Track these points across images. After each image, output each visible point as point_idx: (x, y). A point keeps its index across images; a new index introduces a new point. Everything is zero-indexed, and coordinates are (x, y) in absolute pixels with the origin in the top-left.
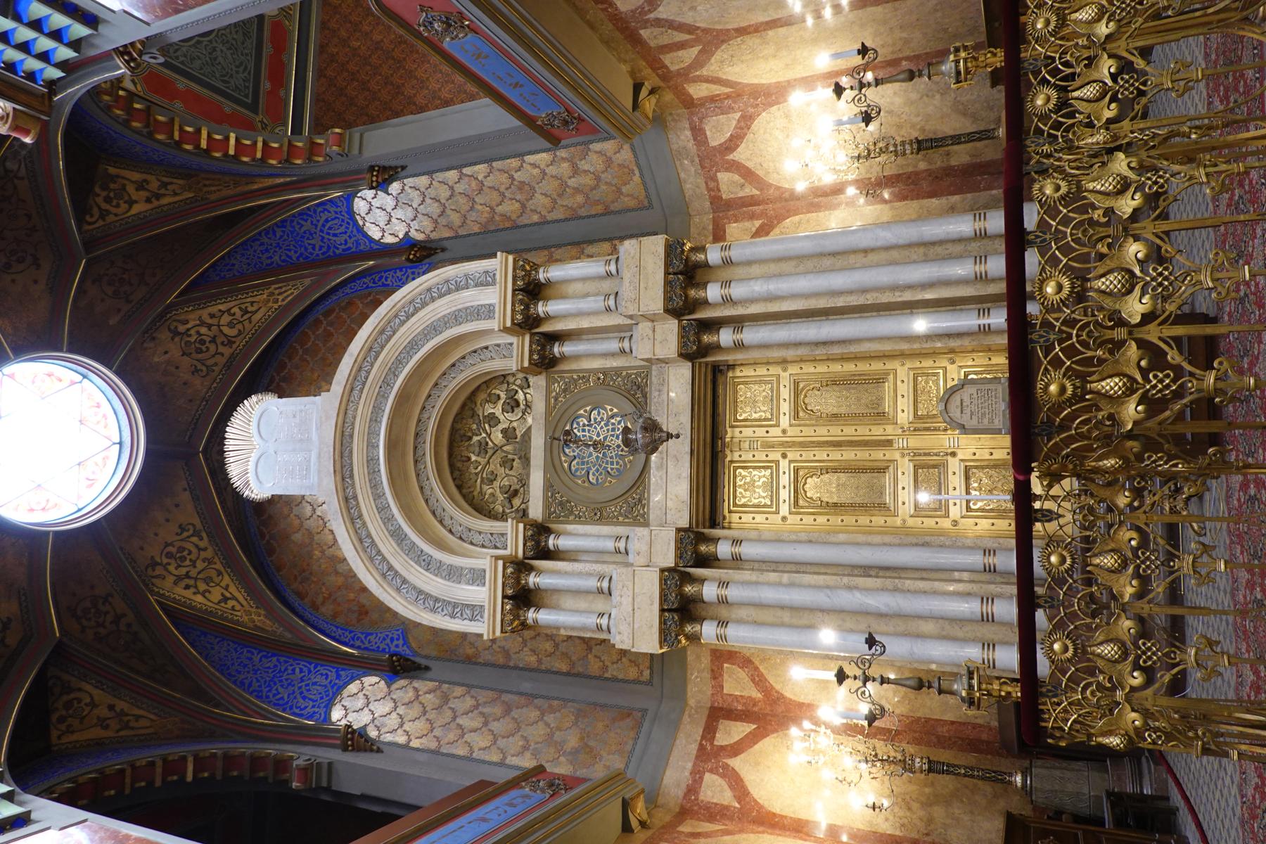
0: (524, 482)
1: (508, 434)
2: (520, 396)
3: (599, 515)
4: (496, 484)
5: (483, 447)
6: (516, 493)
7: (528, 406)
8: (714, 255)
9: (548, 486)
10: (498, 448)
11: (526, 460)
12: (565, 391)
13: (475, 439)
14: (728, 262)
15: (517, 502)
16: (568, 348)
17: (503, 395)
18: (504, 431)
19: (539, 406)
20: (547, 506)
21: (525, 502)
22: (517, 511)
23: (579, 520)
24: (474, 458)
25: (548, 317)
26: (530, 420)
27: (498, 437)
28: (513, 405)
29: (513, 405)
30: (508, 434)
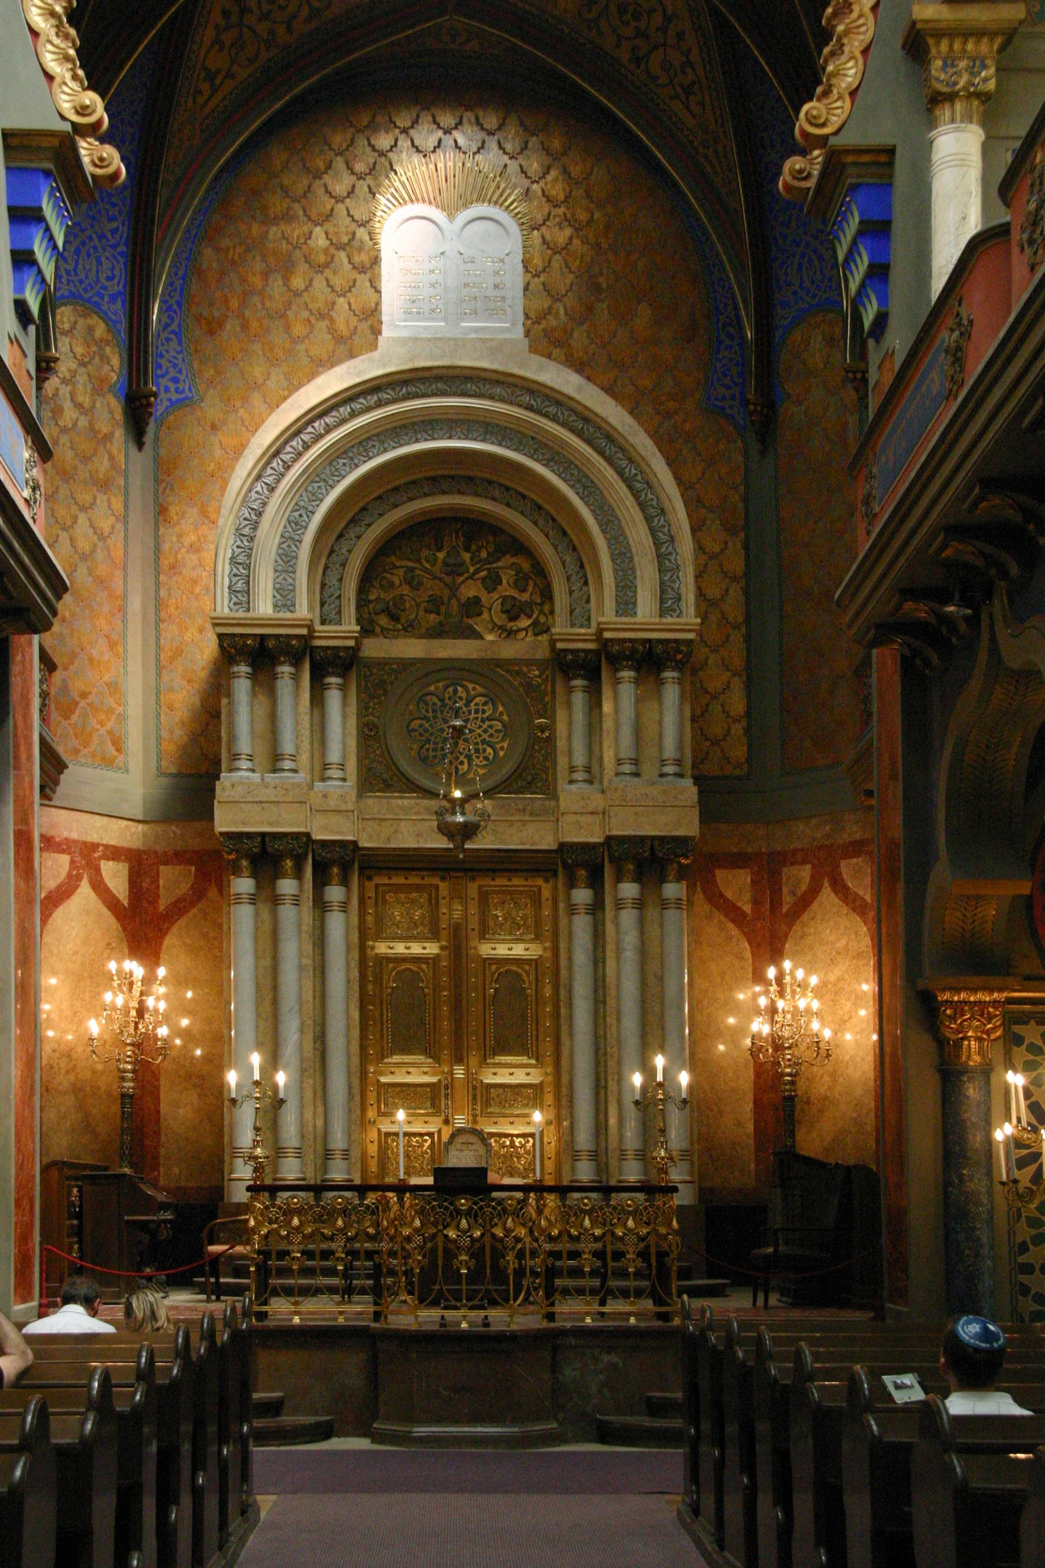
0: (409, 629)
1: (473, 607)
2: (524, 622)
3: (369, 735)
4: (406, 590)
5: (455, 569)
6: (395, 618)
7: (510, 634)
8: (672, 890)
9: (406, 664)
10: (454, 589)
11: (438, 633)
12: (529, 686)
13: (467, 556)
14: (664, 904)
15: (384, 621)
16: (579, 699)
17: (525, 597)
18: (476, 601)
19: (509, 650)
20: (383, 663)
21: (385, 633)
22: (372, 622)
23: (363, 709)
24: (441, 555)
25: (617, 682)
26: (490, 637)
27: (470, 590)
28: (513, 610)
29: (513, 610)
30: (473, 607)
